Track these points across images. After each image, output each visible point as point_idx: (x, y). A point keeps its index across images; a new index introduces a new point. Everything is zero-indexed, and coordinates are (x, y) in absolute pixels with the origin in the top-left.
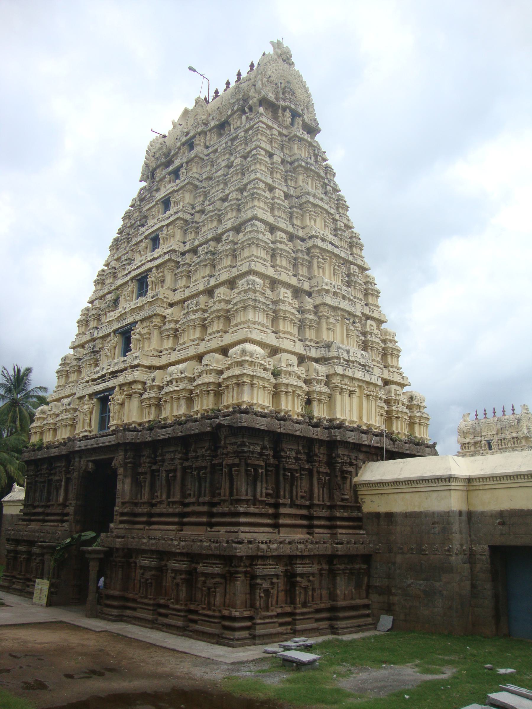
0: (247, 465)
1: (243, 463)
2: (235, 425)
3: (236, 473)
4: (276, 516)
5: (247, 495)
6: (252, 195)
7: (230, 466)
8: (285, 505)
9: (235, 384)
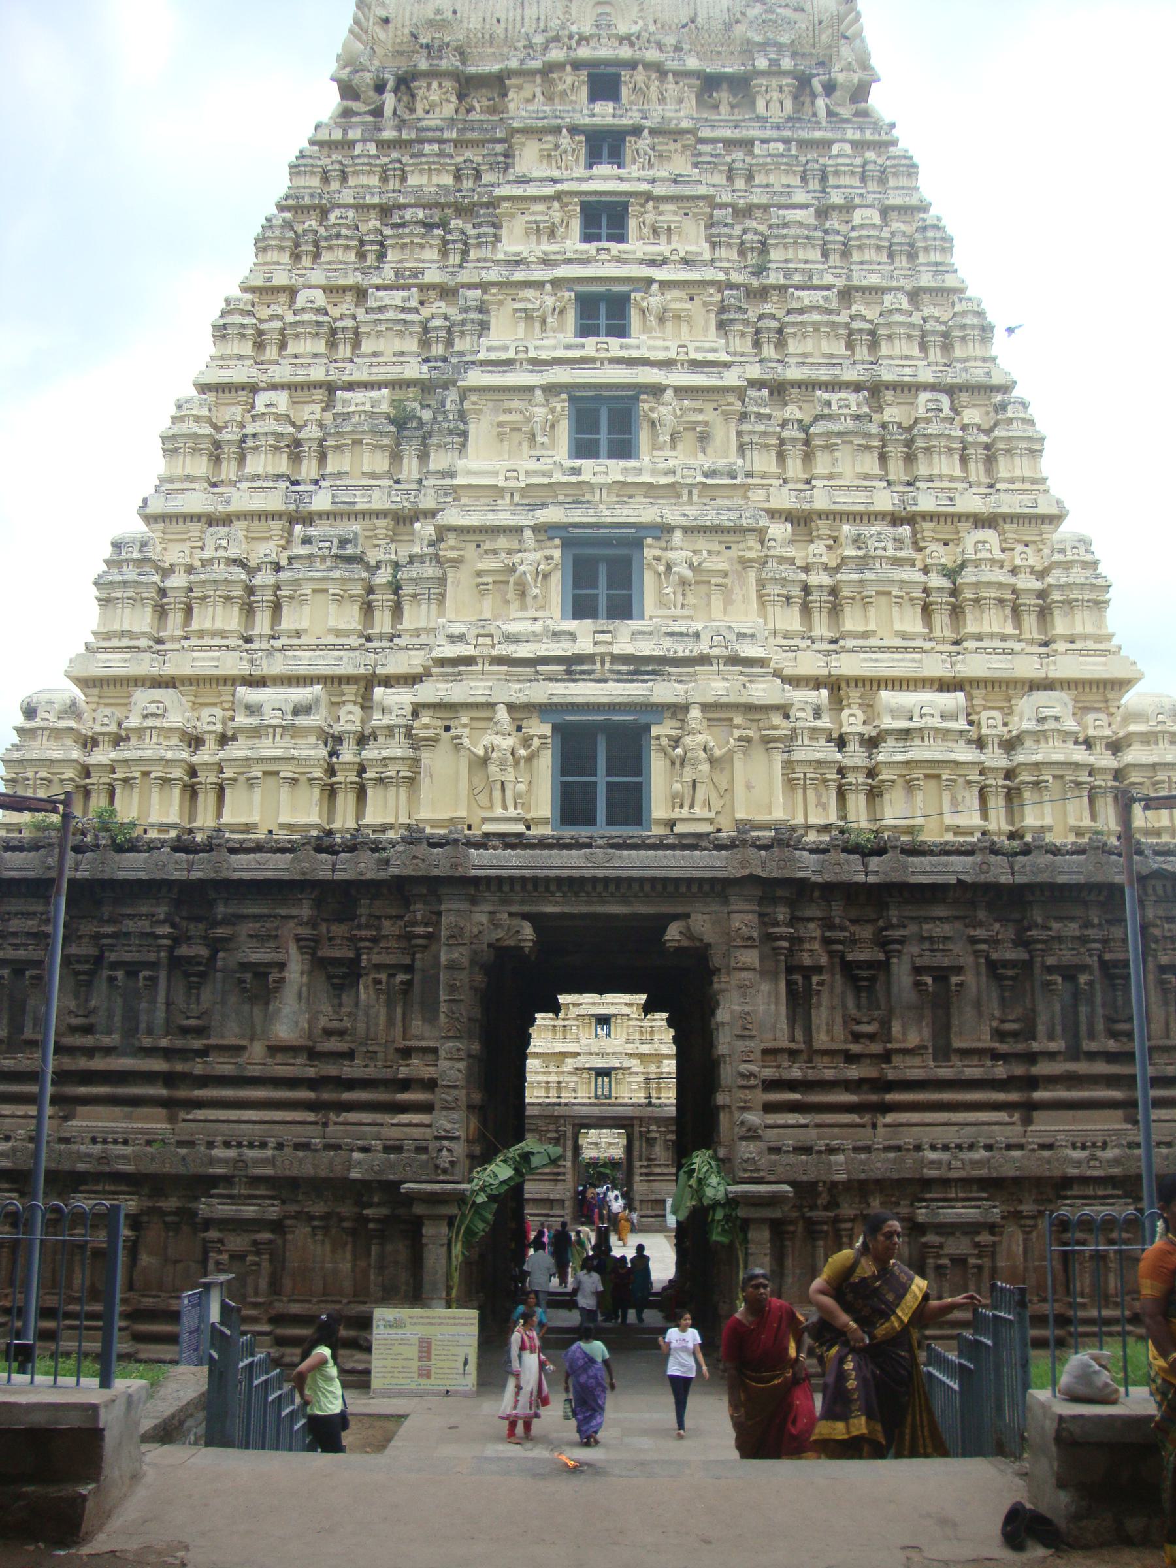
4: (1033, 1083)
8: (1052, 1056)
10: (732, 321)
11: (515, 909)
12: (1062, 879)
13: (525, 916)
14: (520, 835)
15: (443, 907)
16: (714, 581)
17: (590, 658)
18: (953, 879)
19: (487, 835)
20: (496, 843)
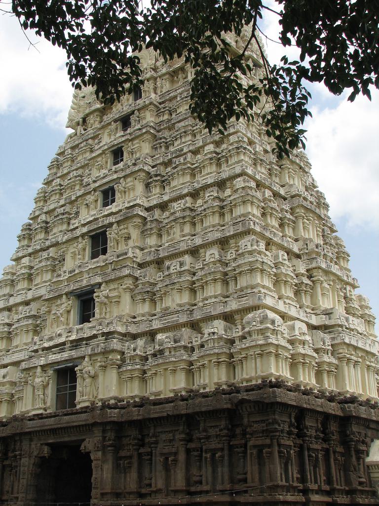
0: (279, 445)
1: (276, 444)
2: (267, 401)
3: (268, 455)
5: (282, 481)
6: (238, 148)
7: (260, 448)
9: (258, 354)
10: (151, 183)
11: (42, 443)
12: (203, 409)
13: (47, 444)
14: (42, 414)
15: (23, 444)
16: (113, 301)
17: (64, 344)
18: (165, 414)
19: (34, 415)
20: (36, 418)
